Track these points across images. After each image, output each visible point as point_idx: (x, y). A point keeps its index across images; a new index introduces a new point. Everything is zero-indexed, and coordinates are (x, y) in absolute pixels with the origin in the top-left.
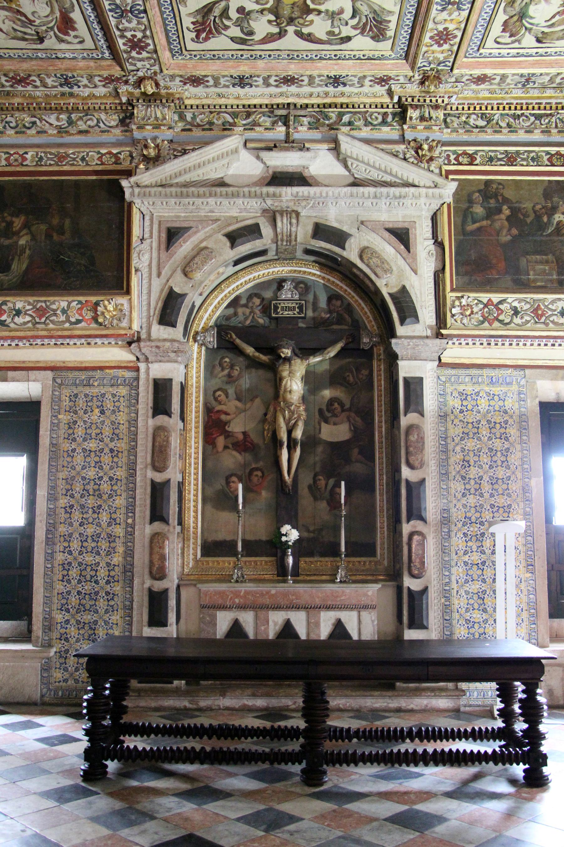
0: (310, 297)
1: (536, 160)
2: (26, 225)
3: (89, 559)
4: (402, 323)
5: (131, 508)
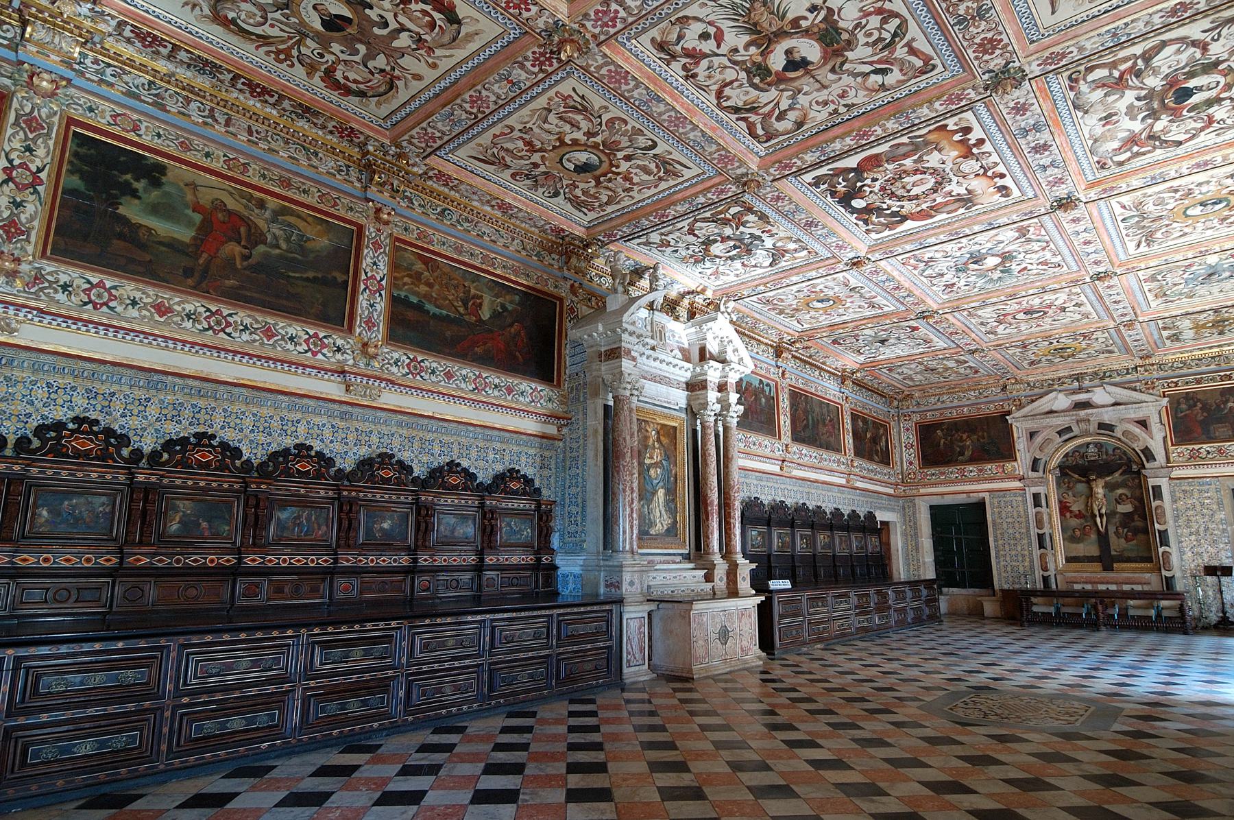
0: (1104, 450)
1: (1213, 380)
2: (968, 437)
3: (1014, 564)
4: (1148, 462)
5: (1030, 544)
